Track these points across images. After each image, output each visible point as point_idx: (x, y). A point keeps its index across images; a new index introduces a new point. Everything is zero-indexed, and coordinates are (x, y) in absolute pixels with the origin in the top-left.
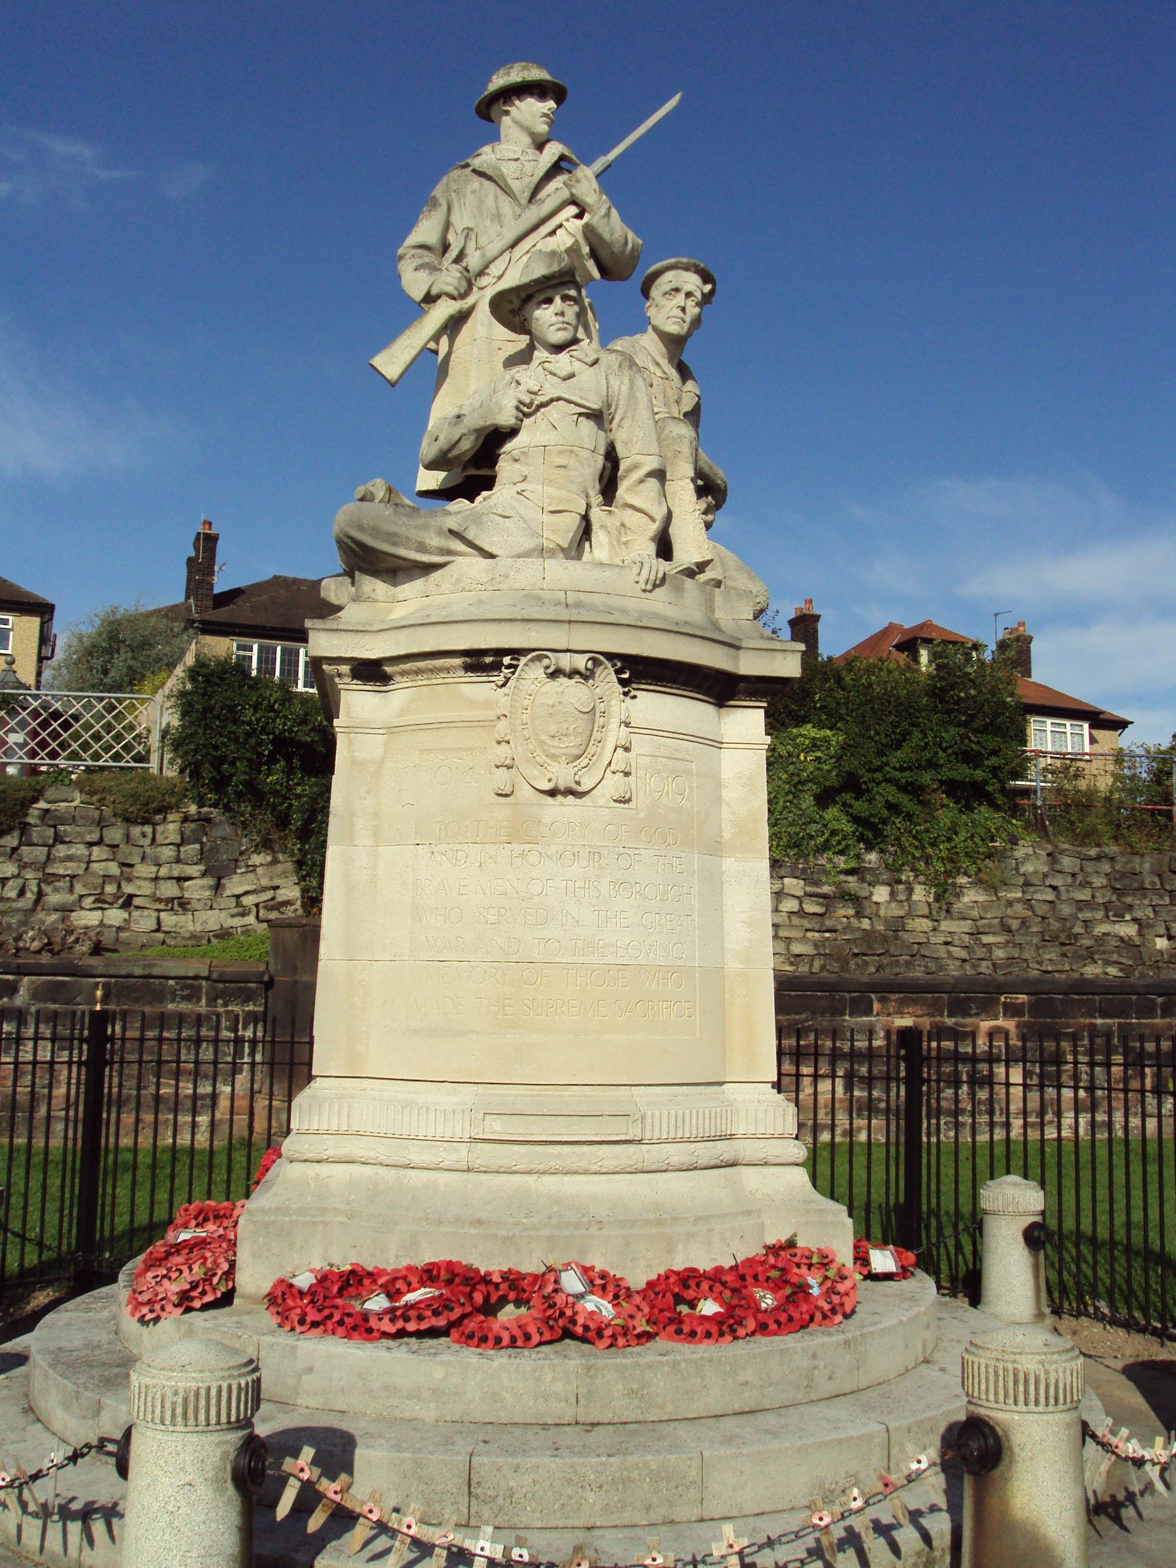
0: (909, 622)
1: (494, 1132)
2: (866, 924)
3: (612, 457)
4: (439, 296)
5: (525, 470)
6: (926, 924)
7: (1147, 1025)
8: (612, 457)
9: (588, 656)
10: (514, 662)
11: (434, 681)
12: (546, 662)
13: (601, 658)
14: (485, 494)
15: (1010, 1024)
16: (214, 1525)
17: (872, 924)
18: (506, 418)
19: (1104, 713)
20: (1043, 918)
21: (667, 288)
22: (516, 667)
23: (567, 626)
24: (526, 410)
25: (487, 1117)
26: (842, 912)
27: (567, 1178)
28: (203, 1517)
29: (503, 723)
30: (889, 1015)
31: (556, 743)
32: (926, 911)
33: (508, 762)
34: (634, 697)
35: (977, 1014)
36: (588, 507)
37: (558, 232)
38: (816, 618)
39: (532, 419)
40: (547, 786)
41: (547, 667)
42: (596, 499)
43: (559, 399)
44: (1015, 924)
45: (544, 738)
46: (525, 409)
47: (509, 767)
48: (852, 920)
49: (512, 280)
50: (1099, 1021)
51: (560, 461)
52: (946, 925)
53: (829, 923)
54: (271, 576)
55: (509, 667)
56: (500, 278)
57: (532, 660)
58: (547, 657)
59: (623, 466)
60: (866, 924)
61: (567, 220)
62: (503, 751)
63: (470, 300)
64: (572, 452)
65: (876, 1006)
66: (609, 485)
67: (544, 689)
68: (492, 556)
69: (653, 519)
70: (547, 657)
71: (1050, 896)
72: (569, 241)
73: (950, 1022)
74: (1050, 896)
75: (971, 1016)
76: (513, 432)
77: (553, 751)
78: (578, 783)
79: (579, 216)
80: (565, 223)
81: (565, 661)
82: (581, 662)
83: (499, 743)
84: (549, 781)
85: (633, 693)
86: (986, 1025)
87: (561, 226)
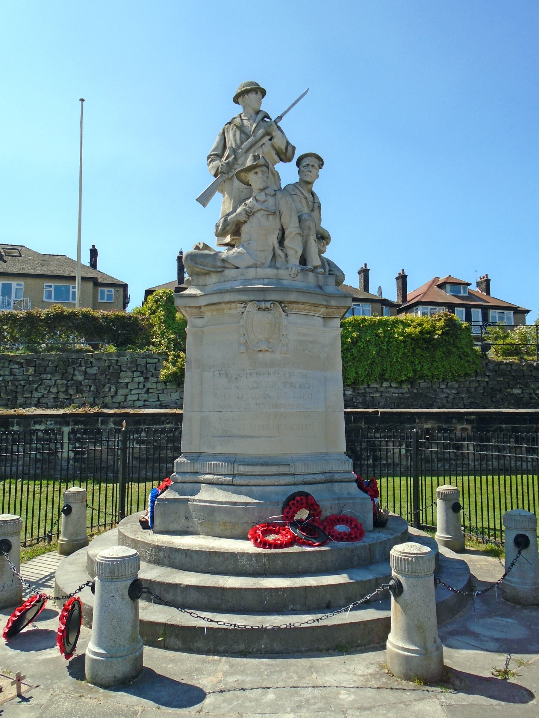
1: (241, 471)
7: (523, 427)
15: (469, 427)
19: (519, 307)
20: (484, 387)
21: (304, 164)
27: (268, 487)
30: (422, 424)
35: (456, 424)
37: (263, 146)
42: (277, 245)
43: (261, 209)
44: (473, 390)
50: (504, 426)
63: (231, 174)
65: (417, 421)
68: (238, 268)
73: (445, 426)
75: (454, 424)
76: (245, 222)
86: (459, 427)
87: (264, 144)
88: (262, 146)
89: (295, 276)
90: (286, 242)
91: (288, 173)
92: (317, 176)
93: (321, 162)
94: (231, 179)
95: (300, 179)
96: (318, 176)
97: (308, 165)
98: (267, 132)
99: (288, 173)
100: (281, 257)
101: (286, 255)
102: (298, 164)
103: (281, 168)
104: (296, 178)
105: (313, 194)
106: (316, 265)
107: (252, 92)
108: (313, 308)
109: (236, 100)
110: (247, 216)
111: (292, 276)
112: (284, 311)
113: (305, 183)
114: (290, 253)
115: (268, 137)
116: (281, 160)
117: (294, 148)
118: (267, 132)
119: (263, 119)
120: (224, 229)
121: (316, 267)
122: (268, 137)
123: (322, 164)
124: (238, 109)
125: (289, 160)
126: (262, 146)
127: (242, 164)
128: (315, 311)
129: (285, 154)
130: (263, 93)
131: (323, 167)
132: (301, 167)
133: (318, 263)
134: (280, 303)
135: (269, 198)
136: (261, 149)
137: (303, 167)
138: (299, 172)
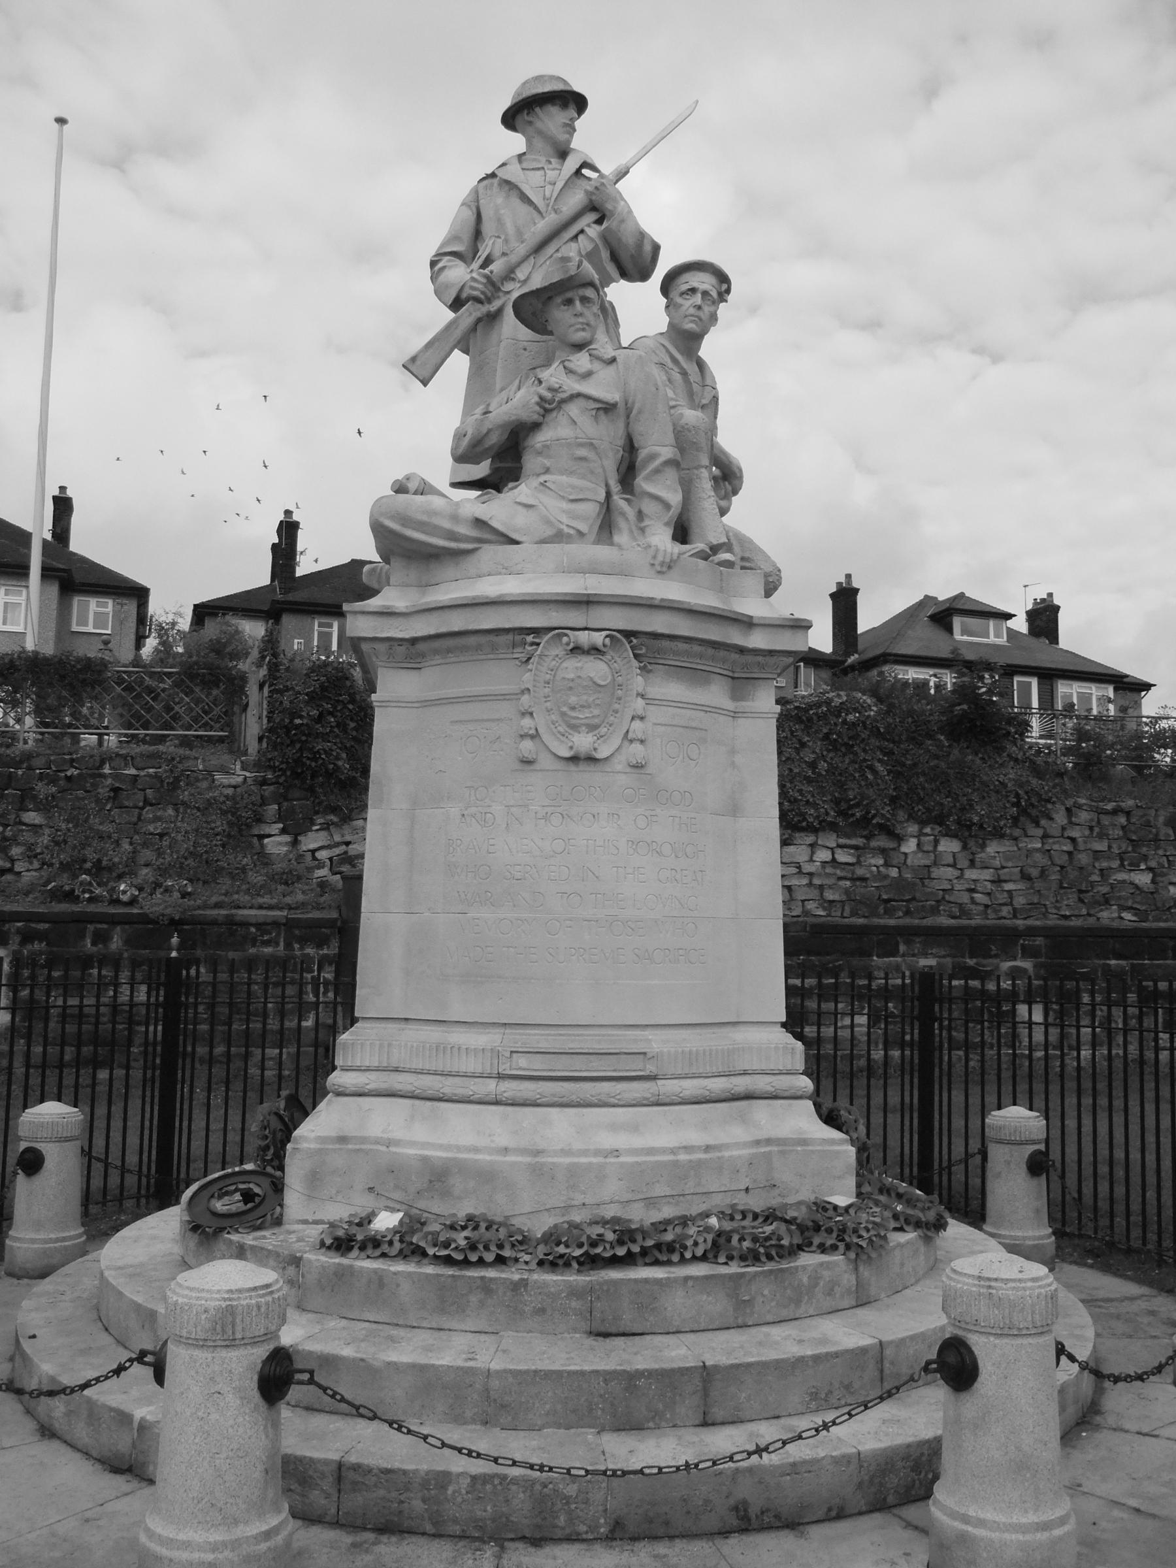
0: (943, 594)
1: (520, 1069)
2: (894, 873)
3: (631, 447)
4: (468, 300)
5: (547, 463)
6: (950, 872)
7: (1159, 966)
8: (631, 447)
9: (604, 633)
10: (537, 640)
11: (462, 659)
12: (565, 639)
13: (618, 635)
14: (511, 485)
15: (1027, 964)
16: (241, 1430)
17: (900, 872)
18: (530, 414)
19: (1127, 676)
20: (1062, 867)
22: (538, 644)
23: (584, 607)
24: (550, 406)
25: (515, 1055)
26: (873, 861)
28: (231, 1422)
29: (525, 698)
30: (913, 955)
31: (573, 714)
32: (950, 860)
33: (532, 732)
34: (649, 671)
35: (996, 956)
36: (608, 495)
37: (581, 237)
38: (857, 590)
39: (554, 414)
40: (568, 754)
41: (568, 644)
42: (615, 487)
43: (579, 395)
44: (1035, 873)
45: (565, 709)
46: (547, 406)
47: (532, 737)
48: (881, 869)
49: (537, 283)
50: (1113, 962)
51: (582, 452)
52: (971, 874)
53: (860, 872)
54: (347, 560)
55: (532, 644)
56: (525, 282)
57: (552, 637)
58: (566, 635)
59: (642, 454)
60: (894, 873)
61: (589, 225)
62: (527, 722)
64: (592, 444)
65: (902, 948)
66: (628, 472)
67: (565, 665)
68: (517, 543)
69: (667, 506)
70: (566, 635)
71: (1068, 847)
72: (590, 247)
73: (971, 962)
74: (1068, 847)
75: (991, 957)
76: (536, 426)
77: (574, 722)
78: (595, 749)
79: (599, 221)
80: (587, 229)
81: (584, 638)
82: (598, 638)
83: (523, 714)
84: (571, 748)
85: (649, 667)
86: (1006, 965)
87: (582, 231)
88: (576, 237)
89: (664, 569)
90: (642, 483)
91: (639, 308)
92: (713, 318)
93: (725, 287)
94: (494, 317)
95: (670, 324)
96: (716, 320)
97: (693, 290)
98: (591, 201)
99: (639, 308)
100: (627, 519)
101: (640, 515)
102: (666, 287)
103: (620, 293)
104: (661, 323)
105: (701, 365)
106: (715, 543)
107: (543, 108)
108: (710, 651)
109: (510, 119)
110: (542, 411)
111: (659, 569)
112: (636, 656)
113: (686, 339)
114: (649, 507)
115: (593, 216)
116: (625, 274)
117: (656, 248)
118: (591, 201)
119: (578, 172)
120: (477, 443)
121: (715, 549)
122: (593, 216)
123: (728, 291)
124: (516, 142)
125: (643, 274)
126: (576, 237)
127: (525, 282)
128: (713, 658)
129: (633, 260)
130: (578, 102)
131: (730, 298)
132: (674, 294)
133: (717, 538)
134: (629, 634)
135: (597, 366)
136: (573, 245)
137: (682, 294)
138: (667, 307)
